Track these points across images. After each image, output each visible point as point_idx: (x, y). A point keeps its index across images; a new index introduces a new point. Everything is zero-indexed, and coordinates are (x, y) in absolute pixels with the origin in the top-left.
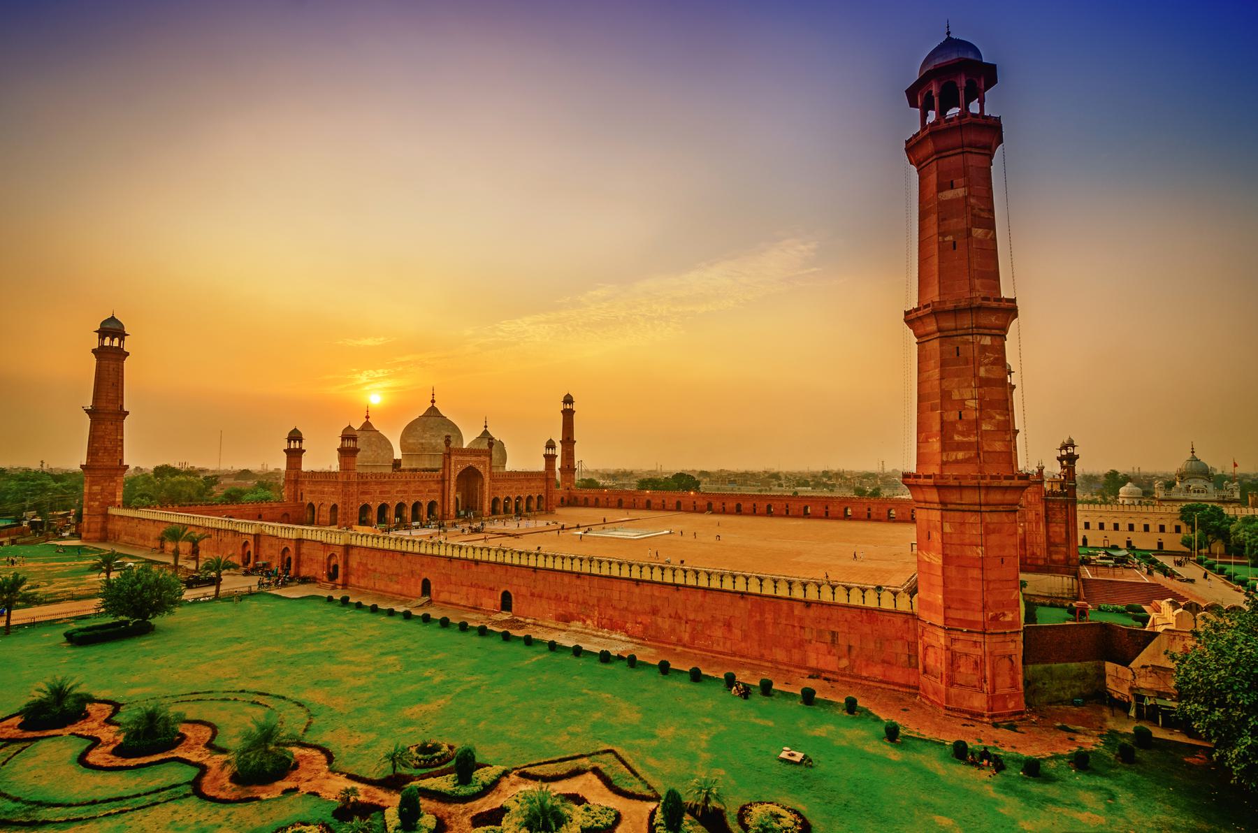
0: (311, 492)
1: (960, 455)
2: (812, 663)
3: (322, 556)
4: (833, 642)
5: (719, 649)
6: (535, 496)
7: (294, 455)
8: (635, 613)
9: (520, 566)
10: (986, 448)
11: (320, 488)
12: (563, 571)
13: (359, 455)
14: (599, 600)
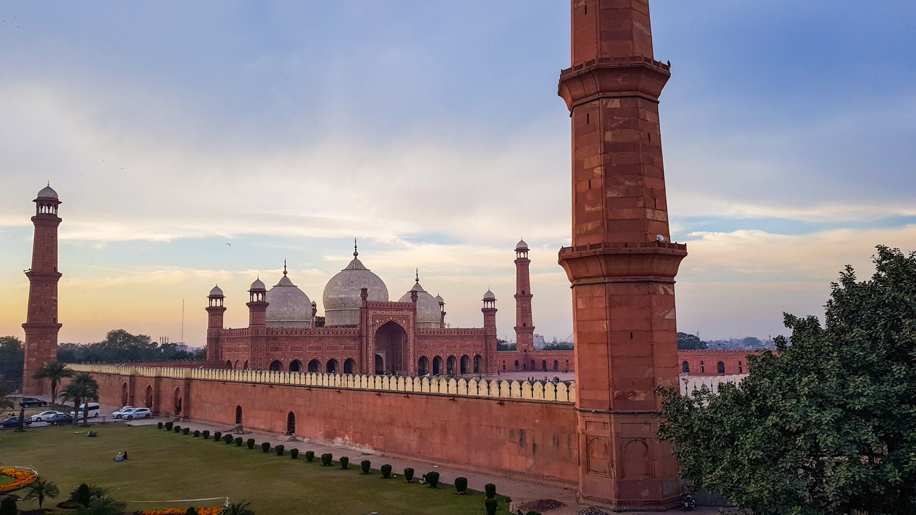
1: (590, 226)
2: (506, 465)
4: (521, 440)
5: (439, 456)
6: (472, 356)
7: (216, 313)
10: (610, 217)
13: (268, 309)
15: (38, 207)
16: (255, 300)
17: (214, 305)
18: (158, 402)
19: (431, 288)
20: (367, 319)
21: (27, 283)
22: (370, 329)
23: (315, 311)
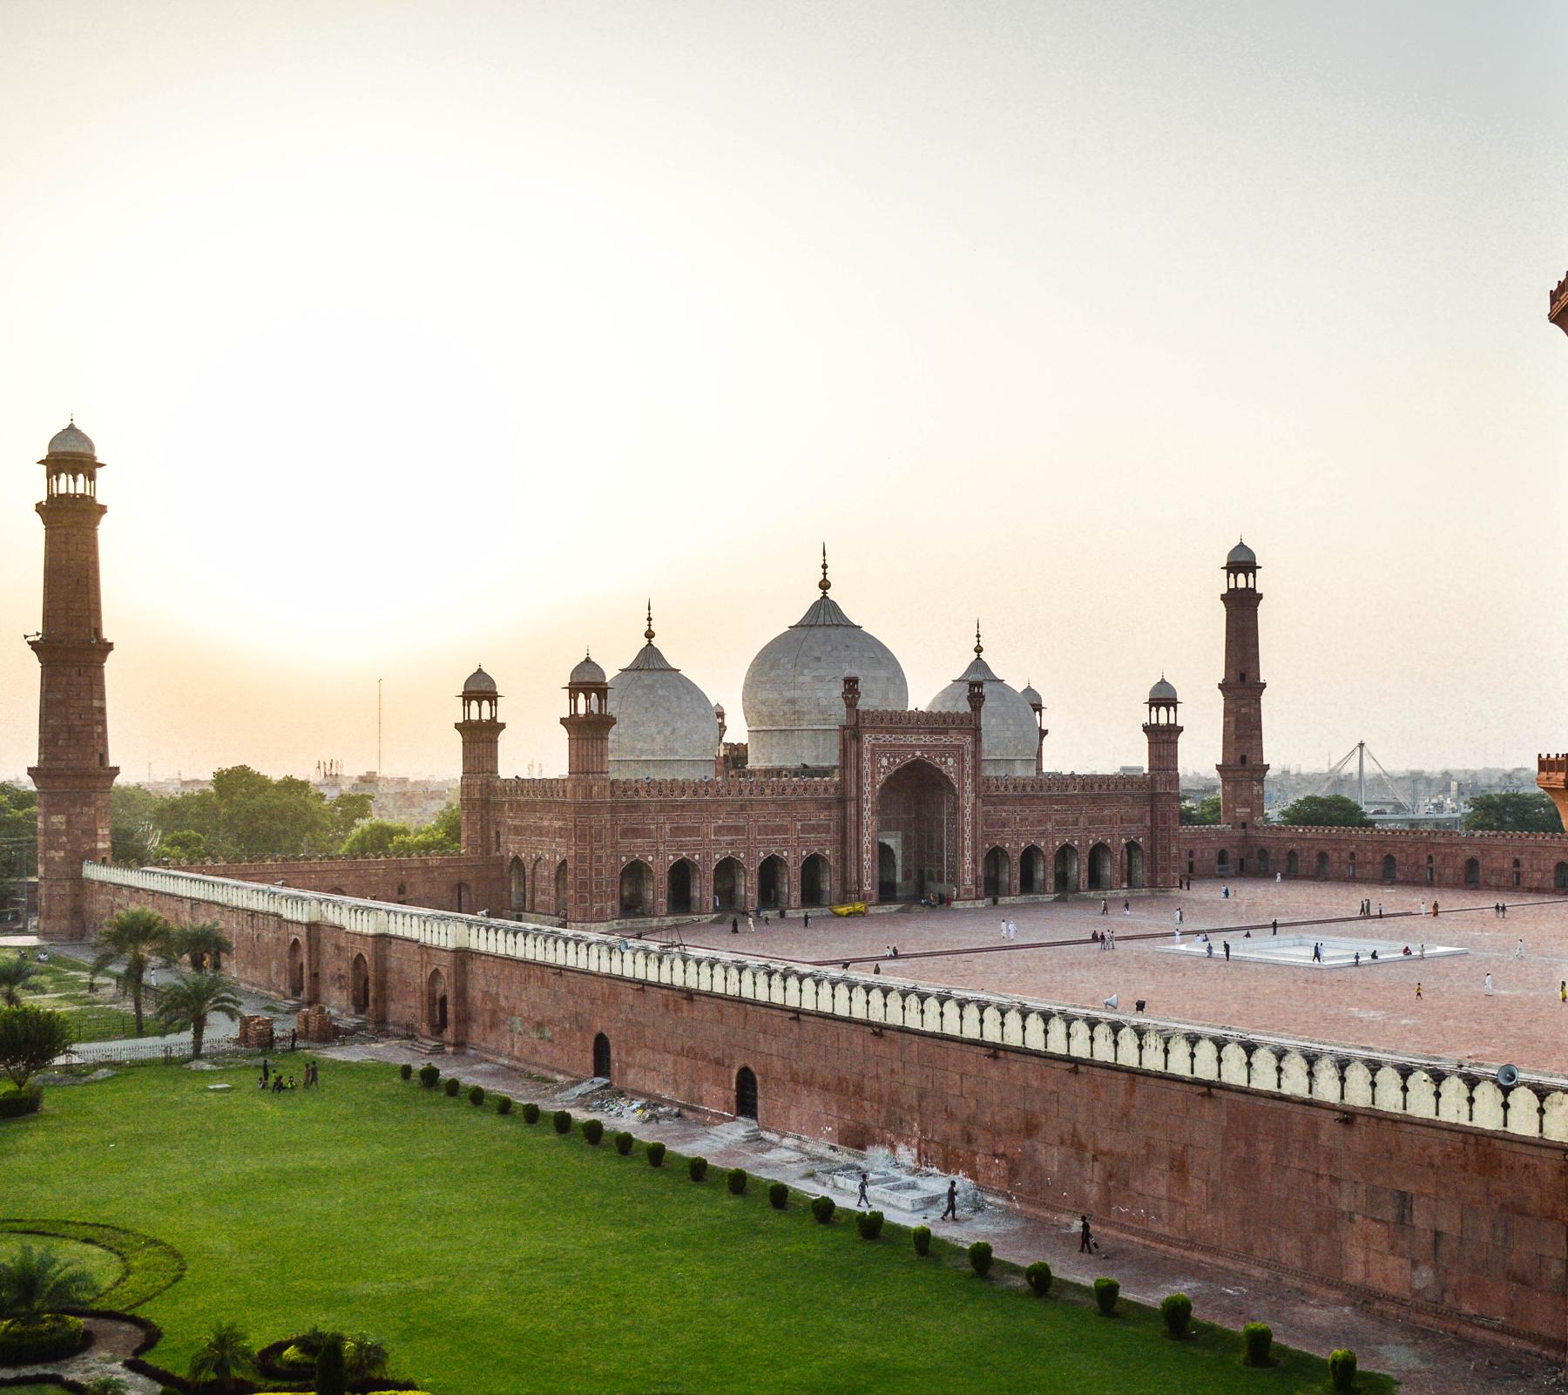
0: (518, 830)
3: (419, 977)
7: (480, 738)
8: (994, 1131)
9: (769, 1006)
11: (531, 820)
12: (849, 1020)
14: (921, 1097)
15: (49, 477)
16: (582, 710)
17: (474, 716)
18: (383, 998)
19: (1012, 672)
20: (859, 755)
21: (32, 667)
22: (867, 781)
23: (722, 728)
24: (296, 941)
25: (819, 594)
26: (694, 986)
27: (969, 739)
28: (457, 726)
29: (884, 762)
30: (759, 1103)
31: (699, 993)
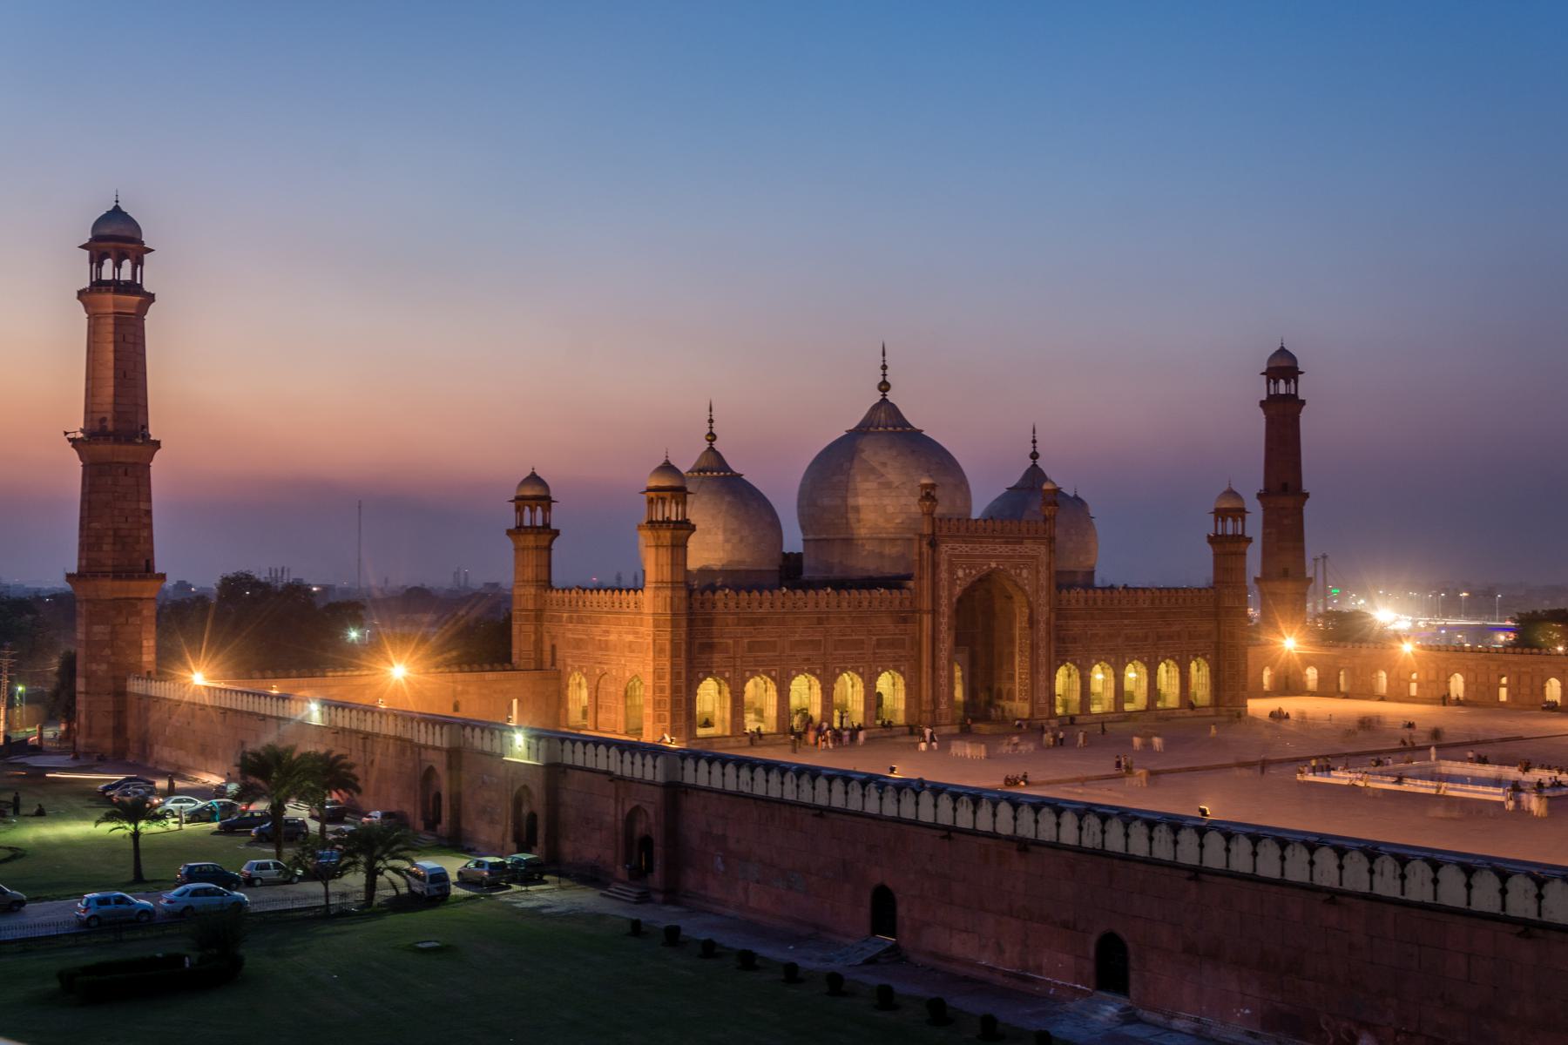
3: (611, 811)
12: (1281, 883)
20: (935, 566)
22: (944, 594)
24: (431, 770)
25: (878, 397)
26: (1031, 835)
27: (1043, 549)
28: (509, 532)
29: (960, 573)
30: (1133, 976)
31: (1037, 843)
